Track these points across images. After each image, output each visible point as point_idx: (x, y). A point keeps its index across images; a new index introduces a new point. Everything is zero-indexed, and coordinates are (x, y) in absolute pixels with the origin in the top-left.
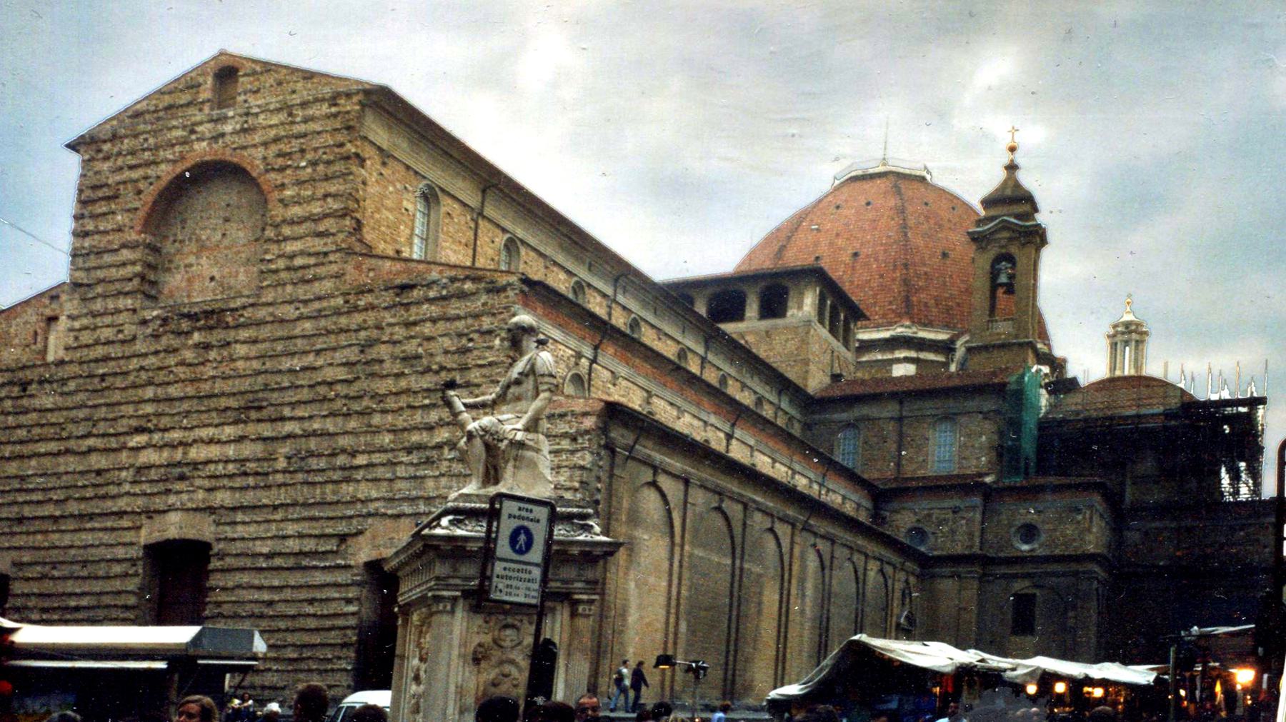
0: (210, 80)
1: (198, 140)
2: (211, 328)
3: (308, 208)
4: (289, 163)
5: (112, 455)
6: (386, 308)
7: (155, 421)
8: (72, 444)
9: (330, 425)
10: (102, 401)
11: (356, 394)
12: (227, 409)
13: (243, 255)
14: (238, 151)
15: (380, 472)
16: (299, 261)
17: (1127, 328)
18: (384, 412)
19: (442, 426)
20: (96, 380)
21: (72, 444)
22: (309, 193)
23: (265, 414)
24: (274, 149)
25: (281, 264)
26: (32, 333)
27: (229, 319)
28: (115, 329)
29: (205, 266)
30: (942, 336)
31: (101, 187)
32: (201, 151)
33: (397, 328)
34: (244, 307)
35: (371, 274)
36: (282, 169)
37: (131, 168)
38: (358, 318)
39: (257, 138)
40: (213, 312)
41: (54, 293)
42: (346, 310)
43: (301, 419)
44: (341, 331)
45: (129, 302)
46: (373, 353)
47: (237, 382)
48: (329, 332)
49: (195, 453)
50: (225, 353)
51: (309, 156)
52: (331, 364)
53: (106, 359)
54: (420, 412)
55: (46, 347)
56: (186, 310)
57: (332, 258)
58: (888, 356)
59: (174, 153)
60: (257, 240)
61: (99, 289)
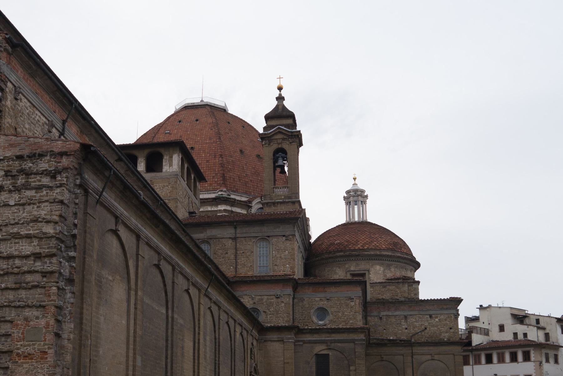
17: (355, 193)
30: (244, 199)
58: (214, 209)
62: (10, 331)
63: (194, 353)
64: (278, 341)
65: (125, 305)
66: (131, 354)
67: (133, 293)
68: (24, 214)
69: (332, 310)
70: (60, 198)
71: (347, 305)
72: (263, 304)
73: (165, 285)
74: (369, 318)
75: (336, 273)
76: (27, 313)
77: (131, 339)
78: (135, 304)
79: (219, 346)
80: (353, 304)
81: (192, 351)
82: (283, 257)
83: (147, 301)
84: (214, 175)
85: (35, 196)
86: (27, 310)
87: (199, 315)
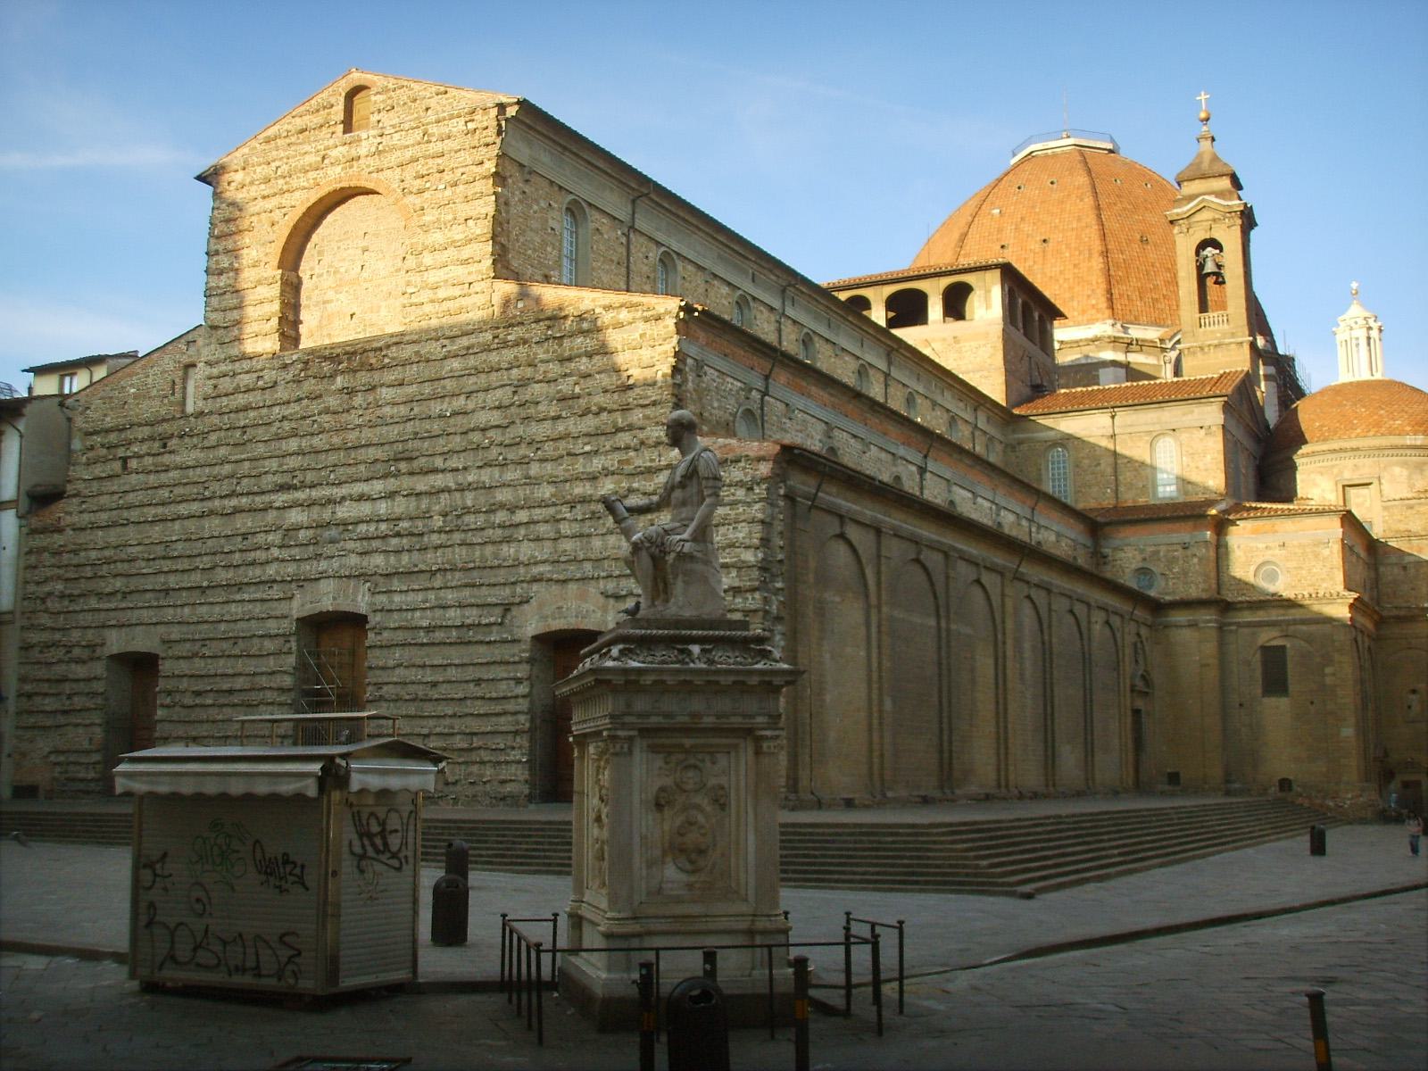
2: (355, 371)
4: (428, 185)
5: (259, 515)
7: (301, 477)
9: (486, 476)
10: (243, 457)
11: (513, 442)
12: (376, 460)
13: (385, 288)
14: (374, 175)
15: (543, 529)
16: (441, 294)
19: (606, 475)
20: (238, 433)
21: (217, 503)
24: (410, 172)
25: (425, 296)
27: (373, 361)
28: (255, 375)
33: (551, 366)
34: (388, 347)
36: (420, 192)
38: (508, 354)
39: (393, 158)
40: (354, 353)
41: (190, 337)
42: (495, 346)
43: (457, 470)
44: (492, 370)
46: (526, 394)
47: (385, 428)
48: (478, 372)
51: (448, 177)
52: (483, 408)
53: (246, 409)
54: (581, 459)
55: (184, 398)
57: (477, 287)
59: (308, 180)
60: (398, 270)
63: (997, 675)
64: (1189, 626)
65: (863, 630)
66: (875, 696)
67: (874, 612)
69: (1290, 565)
70: (760, 516)
71: (1316, 556)
72: (1159, 560)
73: (932, 584)
74: (1382, 569)
75: (1315, 485)
77: (875, 676)
78: (879, 626)
79: (1051, 654)
80: (1326, 552)
81: (992, 671)
82: (1201, 465)
83: (901, 616)
84: (1090, 292)
85: (729, 514)
87: (1003, 612)
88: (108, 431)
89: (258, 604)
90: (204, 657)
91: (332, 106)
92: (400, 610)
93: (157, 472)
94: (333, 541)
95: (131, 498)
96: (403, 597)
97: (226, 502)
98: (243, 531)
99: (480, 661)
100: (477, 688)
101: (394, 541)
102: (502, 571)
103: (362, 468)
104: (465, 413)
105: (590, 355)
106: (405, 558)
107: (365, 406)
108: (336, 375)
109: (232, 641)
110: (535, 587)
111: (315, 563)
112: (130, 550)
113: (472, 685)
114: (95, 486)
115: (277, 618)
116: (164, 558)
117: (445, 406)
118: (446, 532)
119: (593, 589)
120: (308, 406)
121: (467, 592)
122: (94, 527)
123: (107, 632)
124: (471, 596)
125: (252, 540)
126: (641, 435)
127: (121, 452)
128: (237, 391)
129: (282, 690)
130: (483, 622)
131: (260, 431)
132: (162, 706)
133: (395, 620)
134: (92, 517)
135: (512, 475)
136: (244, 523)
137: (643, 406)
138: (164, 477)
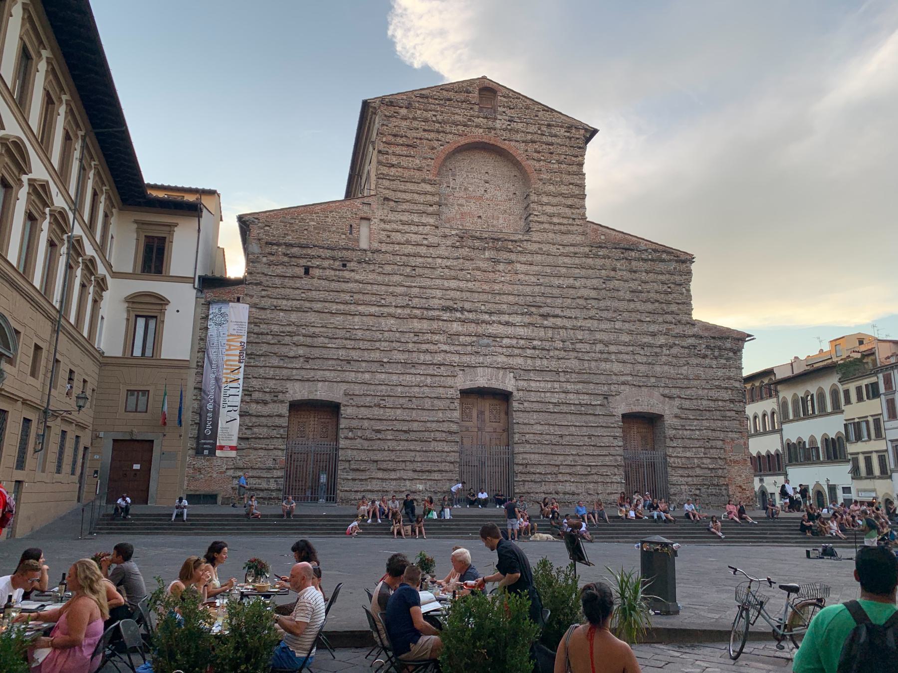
0: (477, 92)
1: (476, 126)
2: (499, 251)
3: (559, 189)
4: (542, 158)
6: (617, 260)
8: (392, 310)
9: (588, 324)
10: (413, 284)
15: (626, 357)
16: (555, 220)
18: (624, 321)
22: (558, 179)
23: (542, 311)
25: (544, 218)
26: (348, 227)
27: (512, 247)
29: (472, 207)
31: (402, 137)
32: (478, 134)
33: (625, 273)
35: (603, 237)
36: (539, 160)
37: (425, 130)
38: (599, 262)
39: (519, 137)
40: (498, 240)
45: (431, 220)
49: (492, 329)
50: (510, 268)
56: (478, 234)
60: (510, 200)
61: (405, 206)
62: (724, 447)
68: (720, 373)
76: (730, 435)
86: (730, 433)
88: (292, 245)
89: (428, 377)
90: (385, 407)
91: (470, 93)
92: (539, 391)
93: (339, 281)
94: (488, 346)
95: (314, 294)
96: (538, 383)
97: (399, 311)
98: (416, 330)
99: (593, 425)
100: (590, 440)
101: (529, 351)
102: (602, 377)
103: (505, 306)
104: (575, 288)
105: (647, 272)
106: (538, 362)
107: (506, 271)
108: (484, 249)
109: (408, 399)
110: (623, 387)
111: (473, 357)
112: (312, 330)
113: (586, 438)
114: (278, 281)
115: (445, 387)
116: (346, 339)
117: (561, 282)
118: (565, 351)
119: (656, 393)
120: (463, 263)
121: (580, 386)
122: (276, 308)
123: (289, 385)
124: (583, 388)
125: (421, 338)
126: (678, 318)
127: (303, 262)
128: (408, 242)
129: (450, 433)
130: (593, 403)
131: (426, 271)
132: (346, 438)
133: (533, 397)
134: (275, 302)
135: (603, 326)
136: (416, 325)
137: (678, 304)
138: (344, 286)
